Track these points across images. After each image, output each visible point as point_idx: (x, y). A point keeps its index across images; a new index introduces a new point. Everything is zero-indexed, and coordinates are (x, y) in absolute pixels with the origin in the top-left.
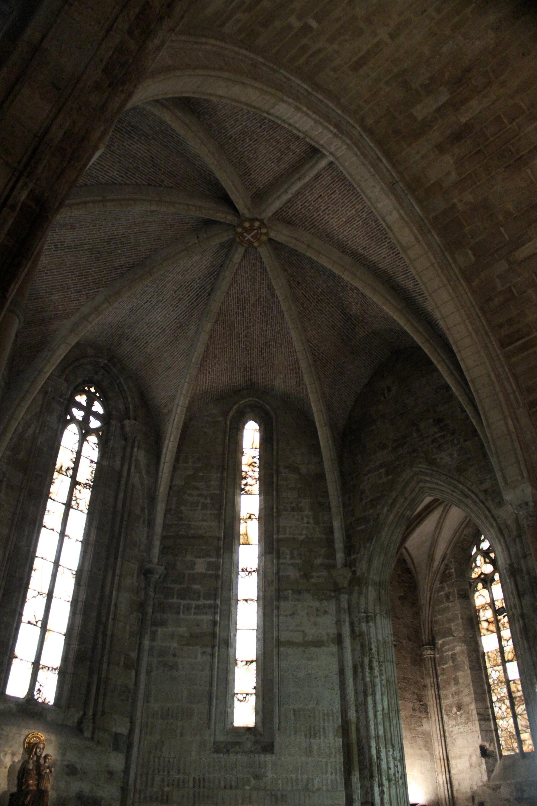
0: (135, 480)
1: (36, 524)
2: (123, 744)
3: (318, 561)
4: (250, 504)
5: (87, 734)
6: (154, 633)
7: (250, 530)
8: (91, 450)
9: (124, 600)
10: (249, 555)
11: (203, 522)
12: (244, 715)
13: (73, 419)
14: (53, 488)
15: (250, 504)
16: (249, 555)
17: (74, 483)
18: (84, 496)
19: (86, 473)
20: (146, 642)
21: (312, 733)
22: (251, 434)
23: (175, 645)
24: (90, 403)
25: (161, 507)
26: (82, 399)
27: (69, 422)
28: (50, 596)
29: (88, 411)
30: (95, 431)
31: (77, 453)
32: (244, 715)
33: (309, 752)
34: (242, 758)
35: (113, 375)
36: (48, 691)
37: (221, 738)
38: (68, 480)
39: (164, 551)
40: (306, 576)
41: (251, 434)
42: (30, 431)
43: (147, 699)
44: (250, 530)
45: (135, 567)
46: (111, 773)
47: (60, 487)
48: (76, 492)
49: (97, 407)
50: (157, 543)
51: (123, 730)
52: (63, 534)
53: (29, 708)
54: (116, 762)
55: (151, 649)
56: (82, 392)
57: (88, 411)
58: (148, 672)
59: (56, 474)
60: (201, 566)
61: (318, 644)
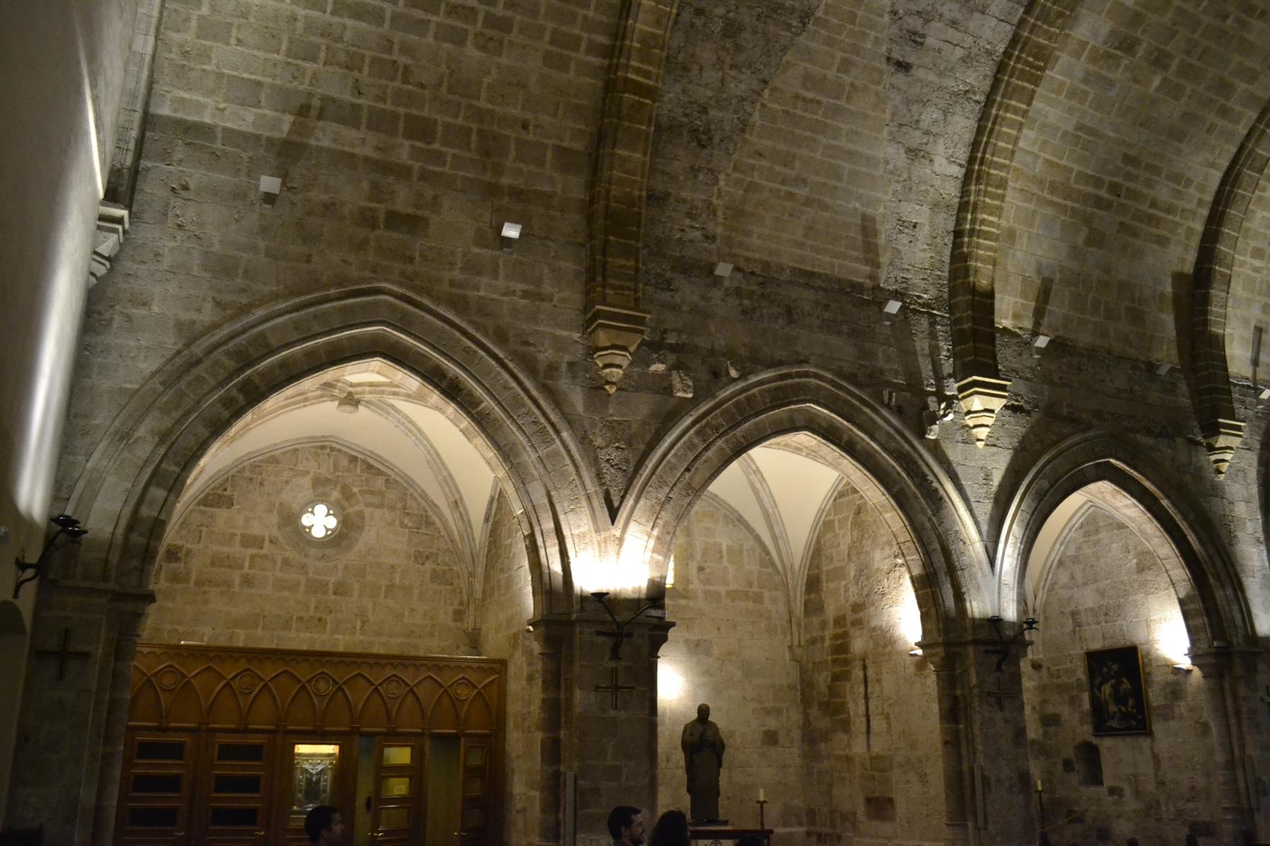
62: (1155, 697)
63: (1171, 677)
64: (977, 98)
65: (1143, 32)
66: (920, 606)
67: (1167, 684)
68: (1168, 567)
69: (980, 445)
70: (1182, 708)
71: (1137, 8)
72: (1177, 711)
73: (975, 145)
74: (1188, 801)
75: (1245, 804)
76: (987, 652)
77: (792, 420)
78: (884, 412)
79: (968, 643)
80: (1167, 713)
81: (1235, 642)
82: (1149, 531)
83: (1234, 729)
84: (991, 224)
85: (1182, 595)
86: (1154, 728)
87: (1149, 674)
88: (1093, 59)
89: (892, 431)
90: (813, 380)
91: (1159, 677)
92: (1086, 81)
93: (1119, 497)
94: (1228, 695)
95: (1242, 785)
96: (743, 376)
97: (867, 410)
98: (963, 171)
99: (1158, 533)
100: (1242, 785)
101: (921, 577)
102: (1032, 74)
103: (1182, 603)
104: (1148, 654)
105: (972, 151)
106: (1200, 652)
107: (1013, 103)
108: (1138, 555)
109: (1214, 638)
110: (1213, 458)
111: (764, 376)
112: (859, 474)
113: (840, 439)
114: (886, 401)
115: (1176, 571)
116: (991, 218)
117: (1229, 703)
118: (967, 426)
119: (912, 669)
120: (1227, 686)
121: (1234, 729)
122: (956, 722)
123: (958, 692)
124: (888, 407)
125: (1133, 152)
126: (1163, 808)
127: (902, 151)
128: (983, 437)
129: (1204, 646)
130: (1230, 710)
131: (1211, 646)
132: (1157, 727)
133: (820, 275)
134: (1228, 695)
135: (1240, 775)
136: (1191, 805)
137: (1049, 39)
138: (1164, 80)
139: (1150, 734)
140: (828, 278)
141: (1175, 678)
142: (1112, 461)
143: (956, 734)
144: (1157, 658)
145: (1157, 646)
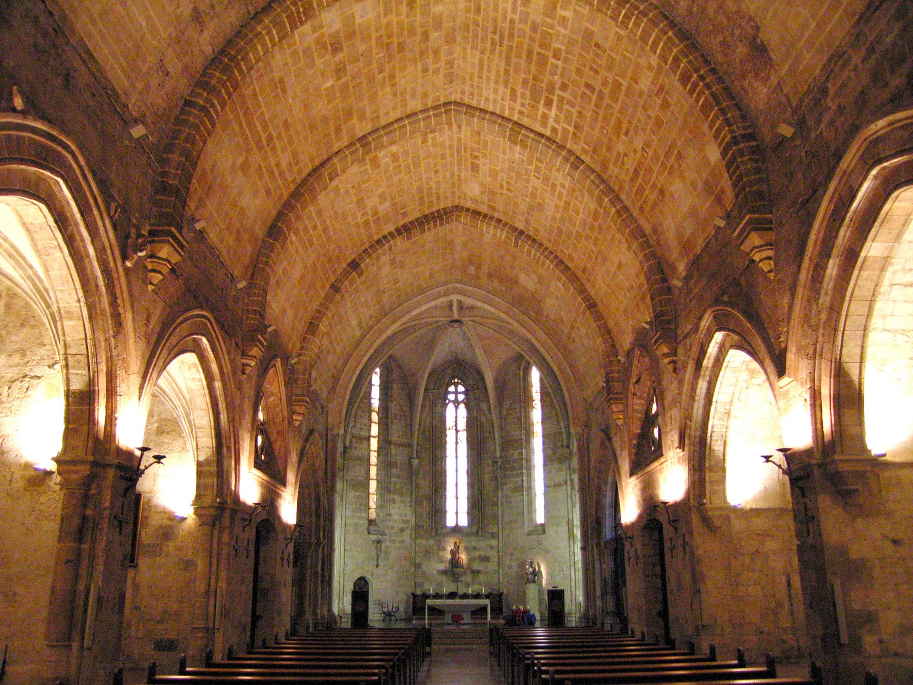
0: (483, 419)
1: (443, 457)
2: (494, 536)
3: (559, 444)
4: (536, 415)
5: (480, 533)
6: (502, 489)
7: (538, 429)
8: (462, 411)
9: (487, 477)
10: (537, 443)
11: (515, 432)
12: (540, 518)
13: (450, 401)
14: (448, 439)
15: (536, 415)
16: (537, 443)
17: (457, 432)
18: (463, 436)
19: (462, 424)
20: (500, 494)
21: (558, 525)
22: (535, 375)
23: (509, 493)
24: (450, 393)
25: (496, 430)
26: (452, 389)
27: (447, 404)
28: (457, 485)
29: (456, 393)
30: (463, 401)
31: (456, 416)
32: (540, 518)
33: (557, 532)
34: (534, 537)
35: (461, 368)
36: (464, 521)
37: (531, 529)
38: (454, 432)
39: (503, 449)
40: (555, 453)
41: (535, 375)
42: (428, 422)
43: (503, 516)
44: (538, 429)
45: (490, 461)
46: (492, 547)
47: (450, 436)
48: (459, 436)
49: (461, 388)
50: (498, 448)
51: (495, 530)
52: (457, 457)
53: (456, 529)
54: (494, 542)
55: (502, 496)
56: (450, 386)
57: (456, 393)
58: (502, 504)
59: (448, 432)
60: (516, 455)
61: (560, 485)
62: (146, 536)
63: (166, 522)
64: (250, 8)
65: (348, 46)
66: (68, 421)
67: (161, 527)
68: (199, 435)
69: (150, 287)
70: (171, 547)
71: (357, 28)
72: (165, 549)
73: (229, 42)
74: (159, 622)
75: (211, 626)
76: (121, 478)
77: (37, 184)
78: (107, 222)
79: (110, 466)
80: (155, 550)
81: (229, 501)
82: (198, 403)
83: (214, 568)
84: (216, 111)
85: (201, 459)
86: (140, 562)
87: (146, 518)
88: (318, 41)
89: (107, 245)
90: (70, 157)
91: (155, 521)
92: (304, 52)
93: (194, 370)
94: (215, 540)
95: (211, 610)
96: (24, 113)
97: (96, 212)
98: (213, 56)
99: (205, 407)
100: (211, 610)
101: (74, 392)
102: (295, 21)
103: (199, 464)
104: (149, 501)
105: (226, 46)
106: (204, 505)
107: (274, 32)
108: (160, 421)
109: (217, 496)
110: (245, 361)
111: (39, 125)
112: (65, 271)
113: (66, 230)
114: (111, 214)
115: (204, 439)
116: (218, 107)
117: (215, 545)
118: (146, 267)
119: (21, 484)
120: (216, 533)
121: (214, 568)
122: (81, 540)
123: (89, 512)
124: (111, 218)
125: (290, 121)
126: (133, 628)
127: (191, 7)
128: (155, 282)
129: (208, 501)
130: (215, 552)
131: (214, 500)
132: (143, 562)
133: (97, 62)
134: (215, 540)
135: (212, 602)
136: (160, 627)
137: (318, 6)
138: (333, 86)
139: (136, 567)
140: (100, 70)
141: (170, 523)
142: (204, 340)
143: (79, 553)
144: (156, 506)
145: (158, 495)
